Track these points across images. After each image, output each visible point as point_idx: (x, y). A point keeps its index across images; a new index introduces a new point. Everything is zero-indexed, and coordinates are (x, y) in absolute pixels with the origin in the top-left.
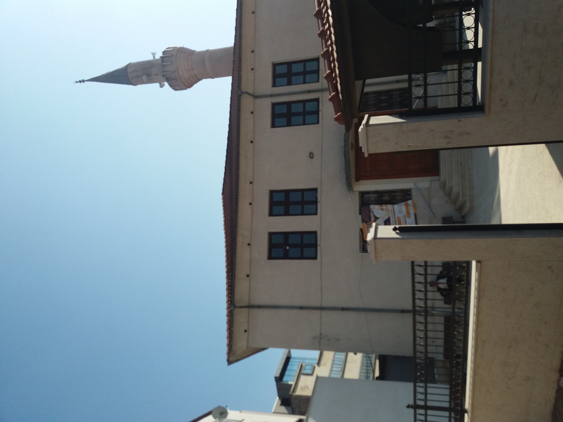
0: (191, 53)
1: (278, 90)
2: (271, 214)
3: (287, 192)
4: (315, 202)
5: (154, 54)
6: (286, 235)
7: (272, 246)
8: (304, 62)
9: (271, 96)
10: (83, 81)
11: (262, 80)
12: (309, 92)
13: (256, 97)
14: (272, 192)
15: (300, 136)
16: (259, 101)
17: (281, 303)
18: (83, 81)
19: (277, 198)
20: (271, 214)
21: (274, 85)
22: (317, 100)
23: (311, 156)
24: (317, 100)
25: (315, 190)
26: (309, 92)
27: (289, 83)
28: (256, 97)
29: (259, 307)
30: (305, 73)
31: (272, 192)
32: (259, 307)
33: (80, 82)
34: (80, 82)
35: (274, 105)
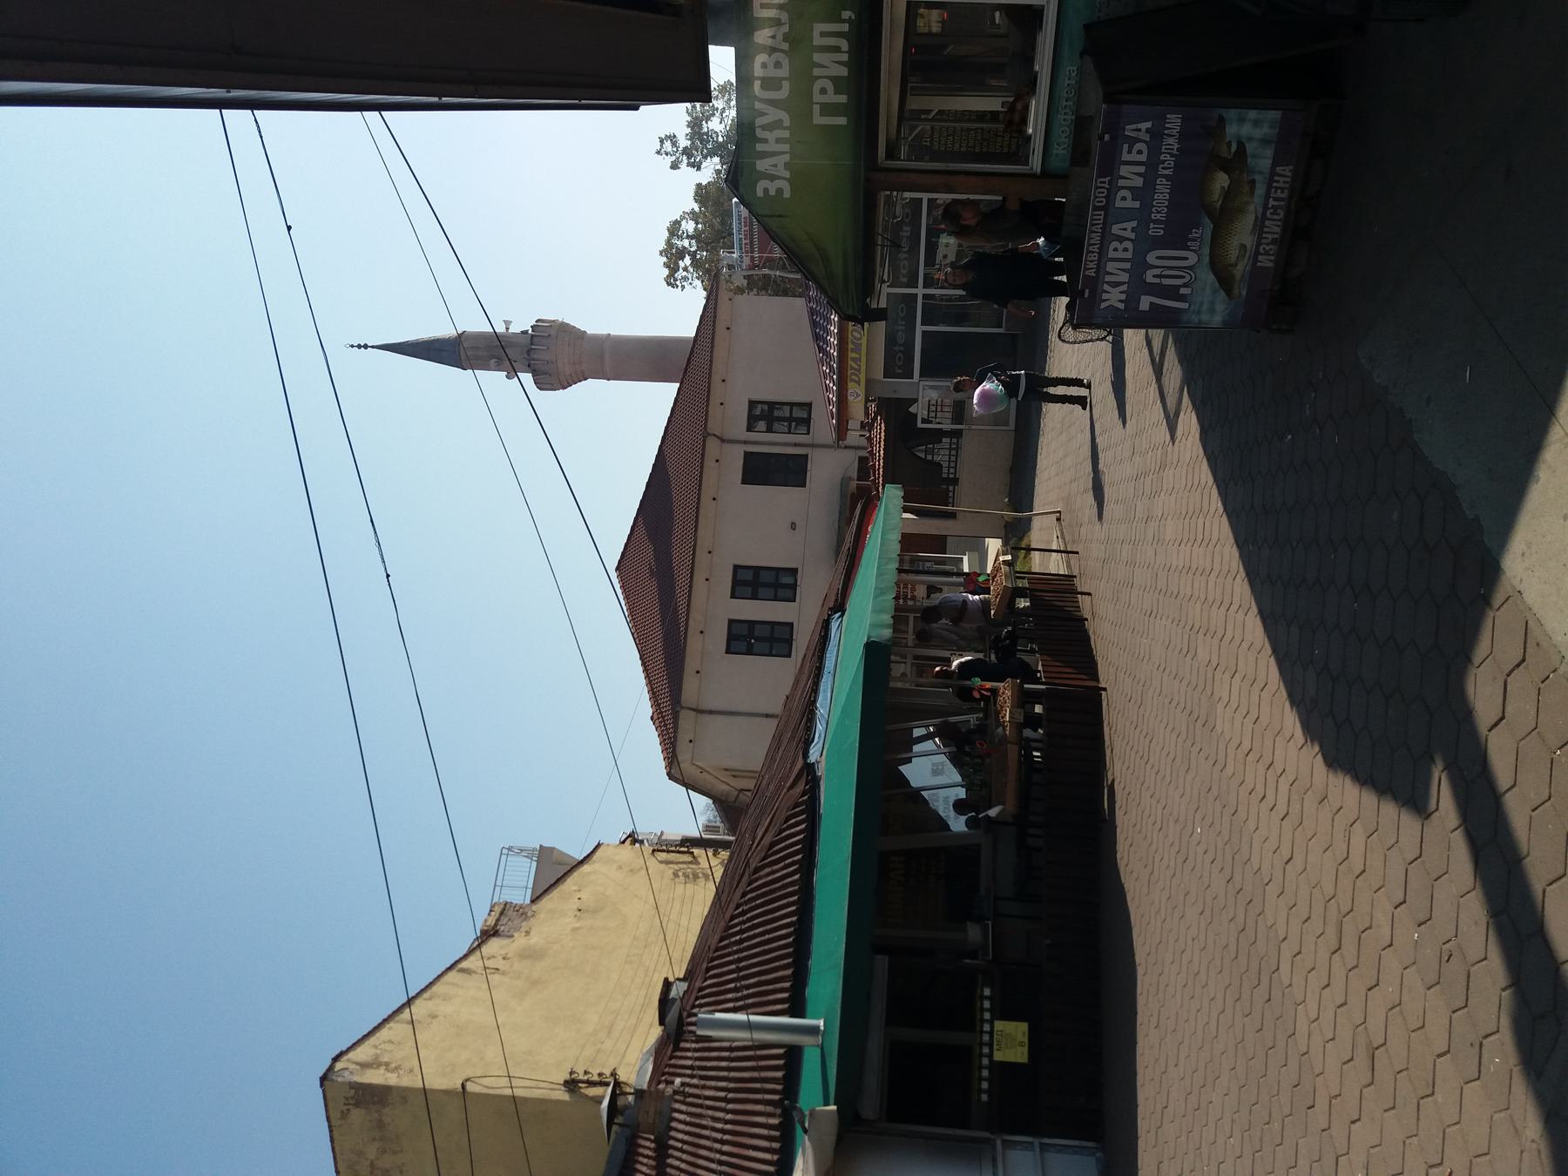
0: (582, 335)
1: (753, 436)
2: (733, 596)
3: (757, 570)
4: (794, 587)
5: (507, 323)
6: (752, 624)
7: (731, 638)
8: (792, 405)
9: (745, 442)
10: (366, 347)
11: (731, 416)
12: (796, 445)
13: (723, 441)
14: (736, 568)
15: (778, 499)
16: (726, 446)
17: (742, 708)
18: (366, 347)
19: (742, 575)
20: (733, 596)
21: (749, 430)
22: (806, 456)
23: (793, 526)
24: (806, 456)
25: (794, 571)
26: (796, 445)
27: (769, 430)
28: (723, 441)
29: (711, 712)
30: (790, 419)
31: (736, 568)
32: (711, 712)
33: (359, 346)
34: (359, 346)
35: (747, 455)
